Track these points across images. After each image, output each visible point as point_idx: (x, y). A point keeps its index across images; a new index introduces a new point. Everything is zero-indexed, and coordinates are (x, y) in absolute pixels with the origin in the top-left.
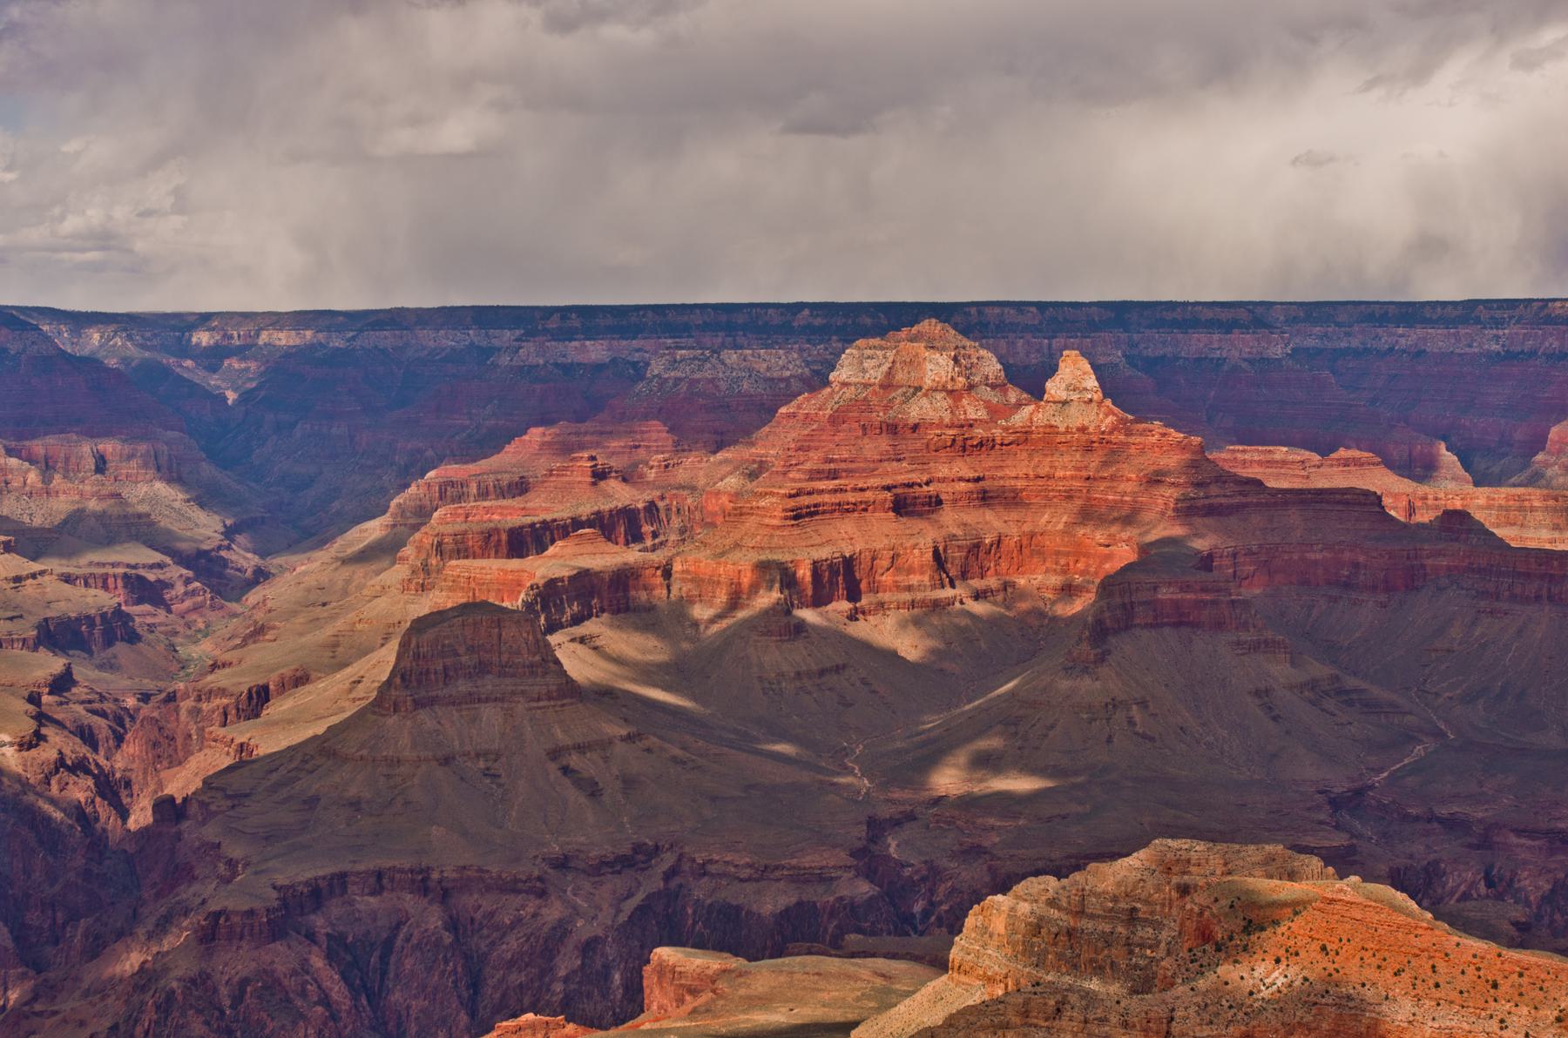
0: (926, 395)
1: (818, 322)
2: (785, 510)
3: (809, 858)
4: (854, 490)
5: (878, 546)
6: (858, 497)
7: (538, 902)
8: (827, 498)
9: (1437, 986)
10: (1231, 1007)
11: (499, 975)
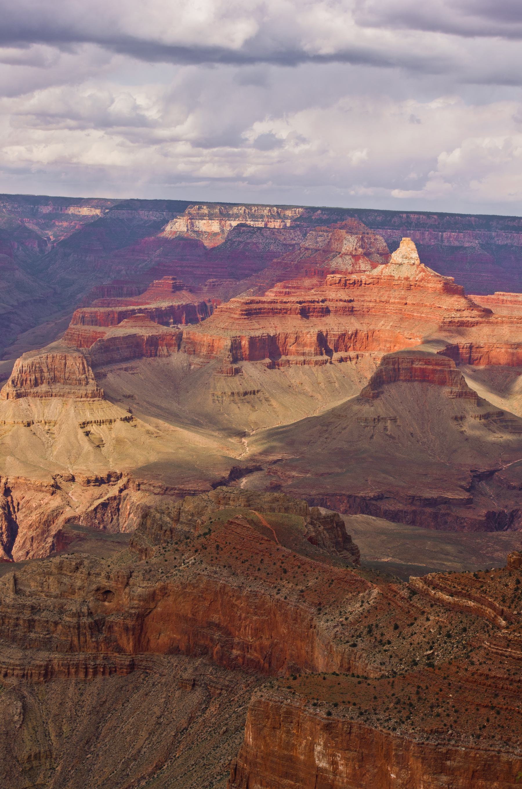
0: (341, 257)
1: (325, 217)
2: (242, 310)
3: (190, 485)
4: (281, 302)
5: (289, 331)
6: (283, 306)
7: (50, 497)
8: (266, 306)
9: (259, 570)
10: (162, 573)
11: (25, 531)
